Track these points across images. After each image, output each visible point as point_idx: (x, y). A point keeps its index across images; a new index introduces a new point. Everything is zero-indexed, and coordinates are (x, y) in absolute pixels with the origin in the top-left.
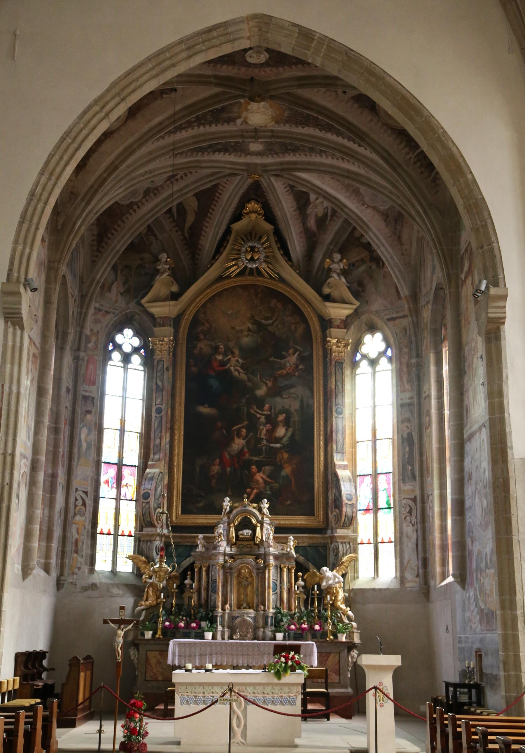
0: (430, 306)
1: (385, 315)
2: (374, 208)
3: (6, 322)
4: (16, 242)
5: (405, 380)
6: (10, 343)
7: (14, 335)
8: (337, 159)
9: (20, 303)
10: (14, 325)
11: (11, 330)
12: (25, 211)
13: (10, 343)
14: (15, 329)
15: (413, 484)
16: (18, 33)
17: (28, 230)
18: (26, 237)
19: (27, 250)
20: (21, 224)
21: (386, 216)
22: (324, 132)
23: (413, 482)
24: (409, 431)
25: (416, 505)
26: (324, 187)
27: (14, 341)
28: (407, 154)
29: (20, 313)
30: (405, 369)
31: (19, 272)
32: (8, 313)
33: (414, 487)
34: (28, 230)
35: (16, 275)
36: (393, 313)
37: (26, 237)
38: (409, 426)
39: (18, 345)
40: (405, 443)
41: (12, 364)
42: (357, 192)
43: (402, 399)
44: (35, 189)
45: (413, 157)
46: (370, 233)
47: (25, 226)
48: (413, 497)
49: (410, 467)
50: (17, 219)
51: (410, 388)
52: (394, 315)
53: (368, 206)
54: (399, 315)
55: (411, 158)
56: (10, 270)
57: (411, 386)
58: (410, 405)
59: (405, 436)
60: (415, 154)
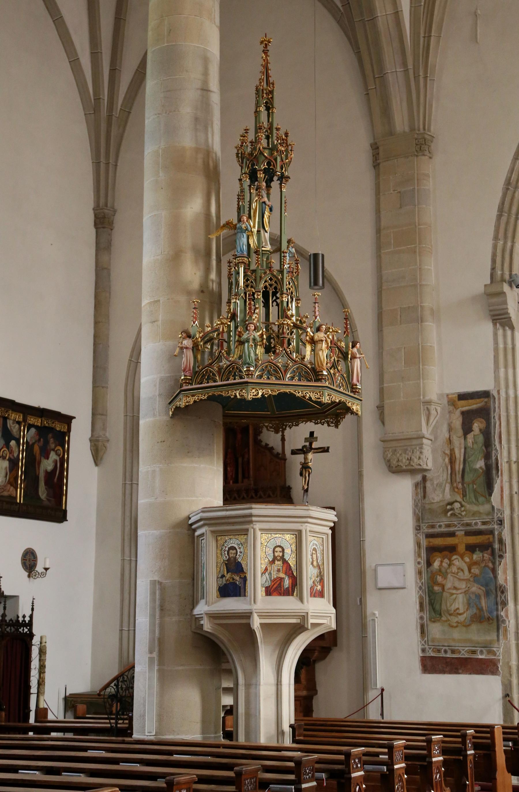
3: (495, 324)
4: (496, 238)
6: (501, 346)
7: (505, 336)
9: (505, 303)
10: (503, 325)
11: (500, 332)
12: (503, 203)
13: (501, 346)
14: (504, 330)
16: (479, 12)
17: (507, 223)
18: (506, 230)
19: (509, 244)
20: (499, 217)
27: (505, 343)
29: (507, 313)
31: (502, 269)
32: (494, 315)
34: (507, 223)
35: (499, 273)
37: (506, 230)
39: (510, 346)
41: (506, 367)
44: (511, 177)
47: (504, 219)
50: (495, 213)
56: (493, 269)
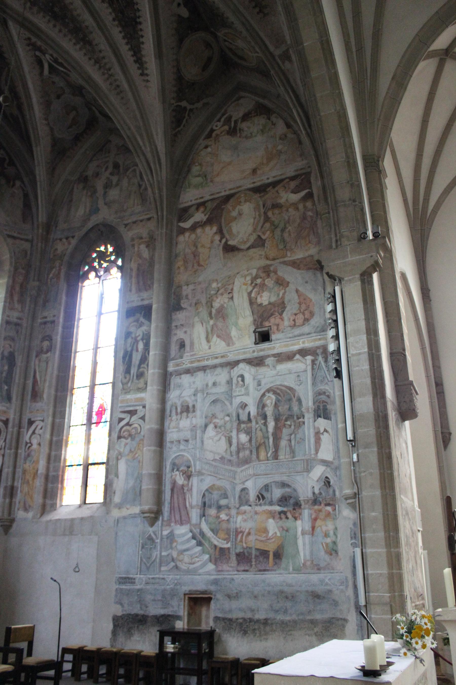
0: (74, 242)
1: (6, 230)
2: (52, 129)
5: (16, 298)
8: (90, 59)
15: (8, 405)
21: (55, 142)
22: (116, 23)
23: (7, 403)
24: (12, 350)
25: (7, 427)
26: (28, 77)
28: (173, 98)
30: (17, 288)
33: (7, 408)
36: (15, 232)
38: (12, 345)
40: (5, 361)
42: (47, 104)
43: (8, 316)
45: (175, 104)
46: (39, 149)
48: (4, 419)
49: (6, 387)
51: (20, 310)
52: (15, 235)
53: (48, 124)
54: (19, 236)
55: (173, 104)
57: (22, 307)
58: (17, 324)
59: (6, 354)
60: (177, 104)
